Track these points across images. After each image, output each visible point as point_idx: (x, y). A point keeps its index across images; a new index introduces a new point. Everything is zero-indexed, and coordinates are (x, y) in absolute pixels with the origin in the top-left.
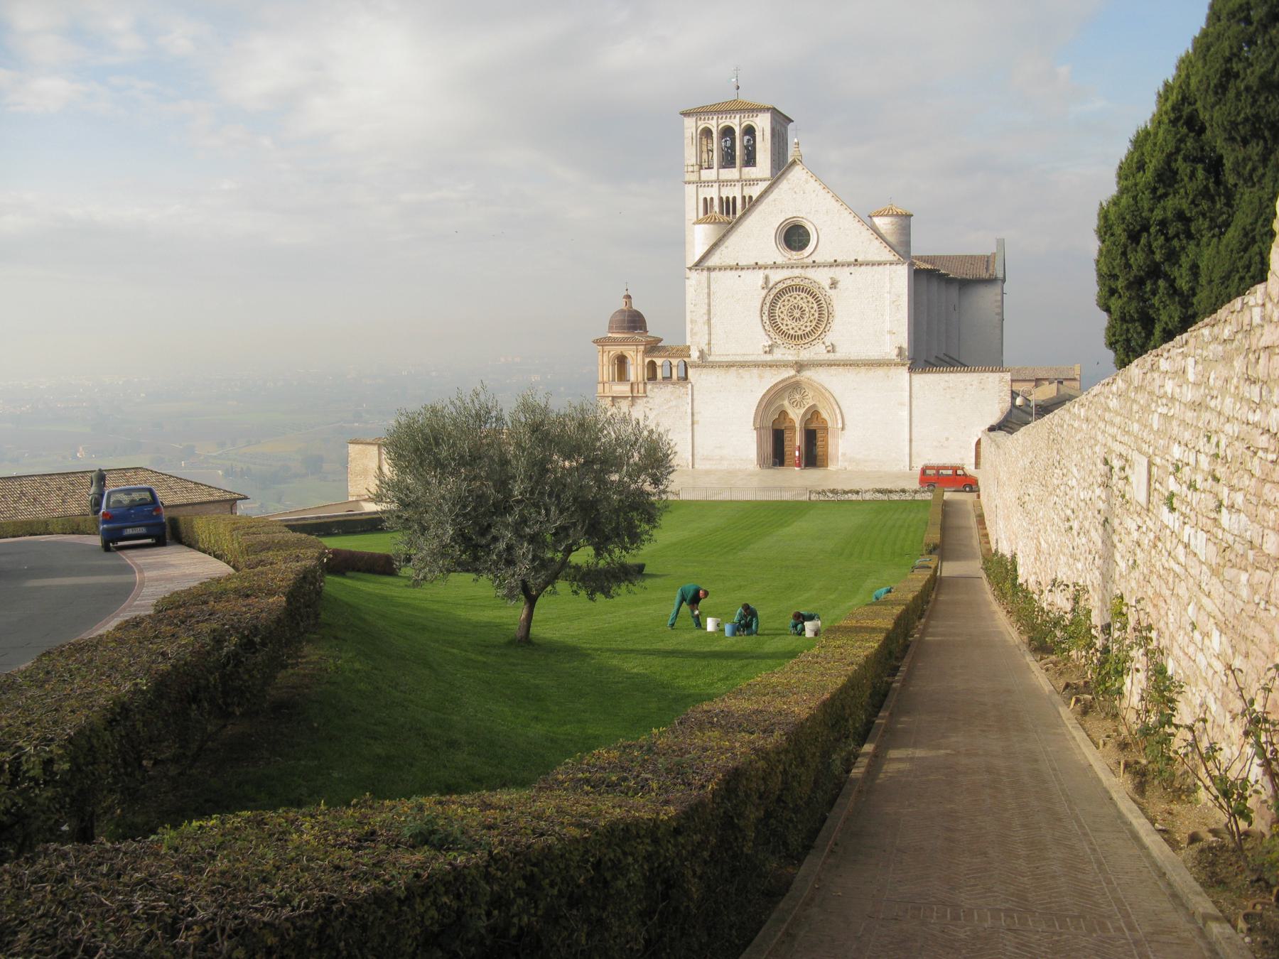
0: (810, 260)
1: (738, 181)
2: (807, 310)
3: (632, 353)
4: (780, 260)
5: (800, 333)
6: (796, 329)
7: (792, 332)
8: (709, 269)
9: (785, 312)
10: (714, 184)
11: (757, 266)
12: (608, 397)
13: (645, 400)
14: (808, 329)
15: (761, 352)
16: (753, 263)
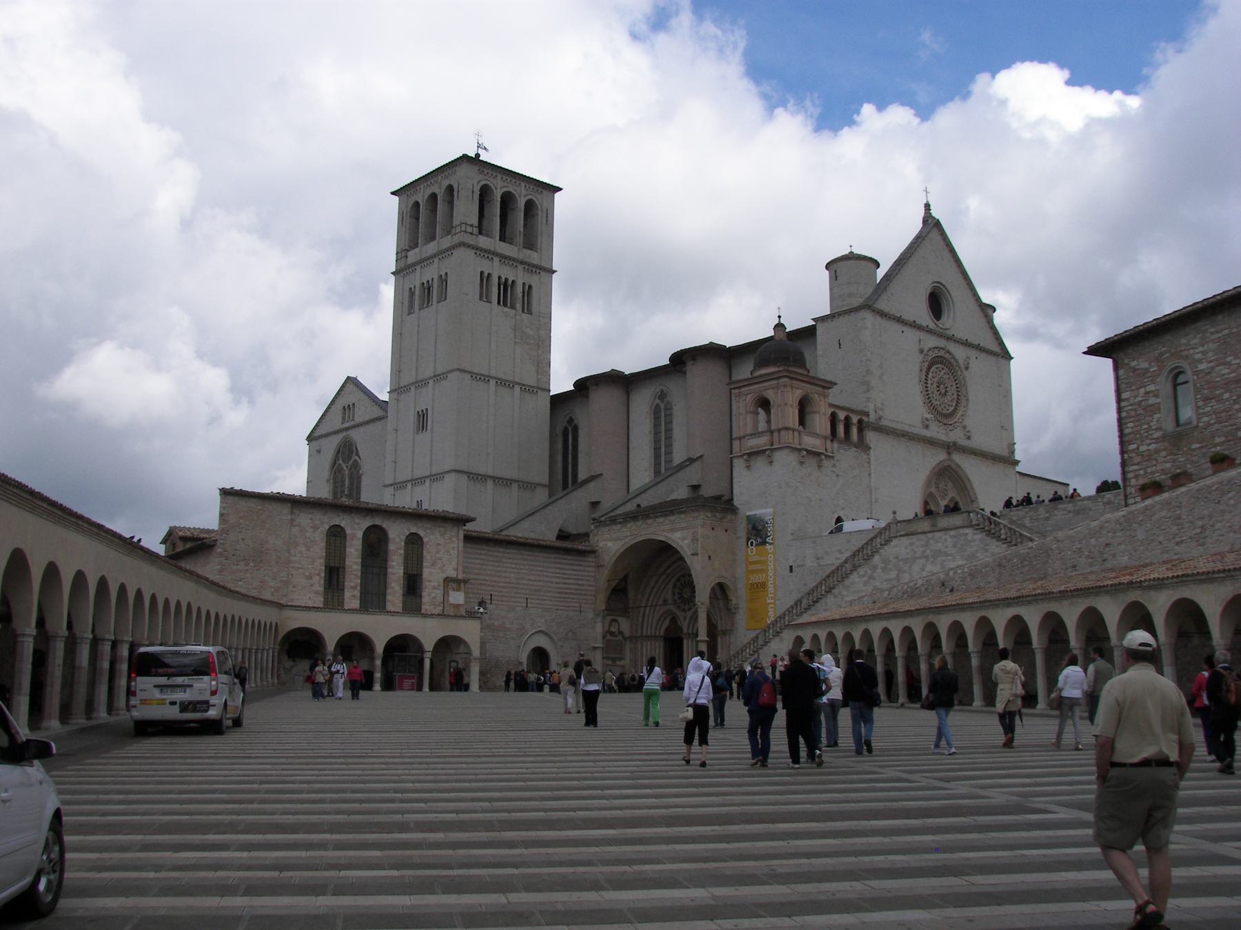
0: (950, 333)
1: (522, 263)
2: (949, 387)
3: (816, 395)
4: (932, 326)
5: (945, 412)
6: (943, 406)
7: (940, 409)
8: (883, 314)
9: (935, 385)
10: (495, 258)
11: (914, 325)
12: (800, 450)
13: (832, 461)
14: (951, 409)
15: (920, 425)
16: (912, 320)
